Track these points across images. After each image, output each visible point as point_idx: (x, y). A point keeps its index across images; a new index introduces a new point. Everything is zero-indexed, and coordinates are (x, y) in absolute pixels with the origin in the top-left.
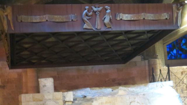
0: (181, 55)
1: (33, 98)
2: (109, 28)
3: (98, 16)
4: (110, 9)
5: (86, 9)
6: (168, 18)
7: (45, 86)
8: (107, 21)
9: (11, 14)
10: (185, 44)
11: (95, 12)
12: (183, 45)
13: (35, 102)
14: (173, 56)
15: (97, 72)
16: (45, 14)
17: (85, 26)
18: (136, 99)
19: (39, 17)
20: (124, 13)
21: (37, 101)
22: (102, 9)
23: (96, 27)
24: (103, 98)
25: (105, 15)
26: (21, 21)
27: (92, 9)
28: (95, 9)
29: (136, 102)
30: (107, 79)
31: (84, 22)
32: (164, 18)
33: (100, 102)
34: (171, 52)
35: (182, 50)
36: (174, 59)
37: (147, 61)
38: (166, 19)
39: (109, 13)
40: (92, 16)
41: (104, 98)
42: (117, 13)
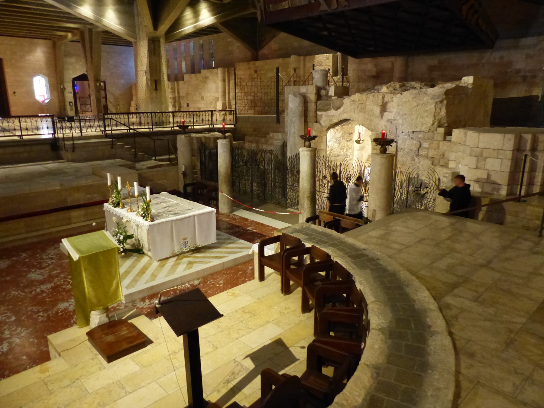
30: (509, 70)
33: (352, 99)
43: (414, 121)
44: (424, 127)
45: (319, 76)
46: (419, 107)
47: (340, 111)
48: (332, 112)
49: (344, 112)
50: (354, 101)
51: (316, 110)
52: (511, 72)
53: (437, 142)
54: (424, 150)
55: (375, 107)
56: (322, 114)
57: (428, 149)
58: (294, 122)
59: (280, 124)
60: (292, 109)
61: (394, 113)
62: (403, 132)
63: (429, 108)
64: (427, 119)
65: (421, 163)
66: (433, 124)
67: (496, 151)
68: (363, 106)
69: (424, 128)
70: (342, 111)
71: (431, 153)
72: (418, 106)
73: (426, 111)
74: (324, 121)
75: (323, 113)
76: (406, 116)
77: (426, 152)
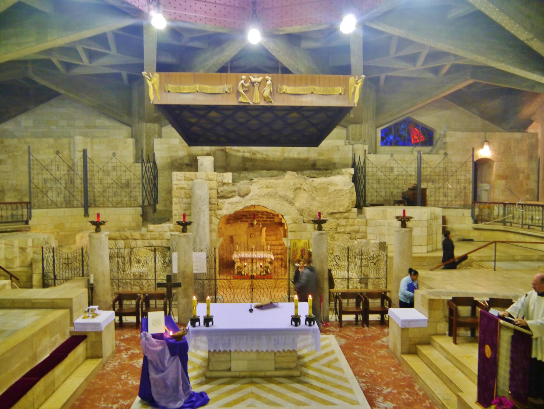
1: (185, 177)
2: (268, 102)
3: (256, 89)
4: (271, 81)
5: (242, 80)
6: (343, 94)
7: (202, 164)
8: (266, 93)
9: (158, 83)
11: (253, 83)
13: (186, 181)
16: (195, 84)
17: (241, 99)
19: (188, 86)
20: (288, 85)
21: (189, 180)
22: (262, 80)
23: (254, 101)
25: (265, 86)
26: (169, 91)
27: (250, 79)
28: (253, 79)
31: (238, 94)
32: (337, 93)
34: (386, 138)
38: (340, 94)
39: (269, 85)
40: (248, 87)
42: (279, 85)
47: (247, 197)
48: (237, 199)
51: (218, 197)
52: (307, 165)
53: (353, 220)
54: (341, 228)
56: (224, 202)
57: (345, 226)
58: (204, 211)
59: (88, 216)
60: (201, 196)
63: (344, 193)
65: (340, 239)
66: (348, 206)
67: (417, 222)
69: (341, 209)
71: (348, 229)
73: (342, 195)
75: (227, 201)
77: (343, 230)
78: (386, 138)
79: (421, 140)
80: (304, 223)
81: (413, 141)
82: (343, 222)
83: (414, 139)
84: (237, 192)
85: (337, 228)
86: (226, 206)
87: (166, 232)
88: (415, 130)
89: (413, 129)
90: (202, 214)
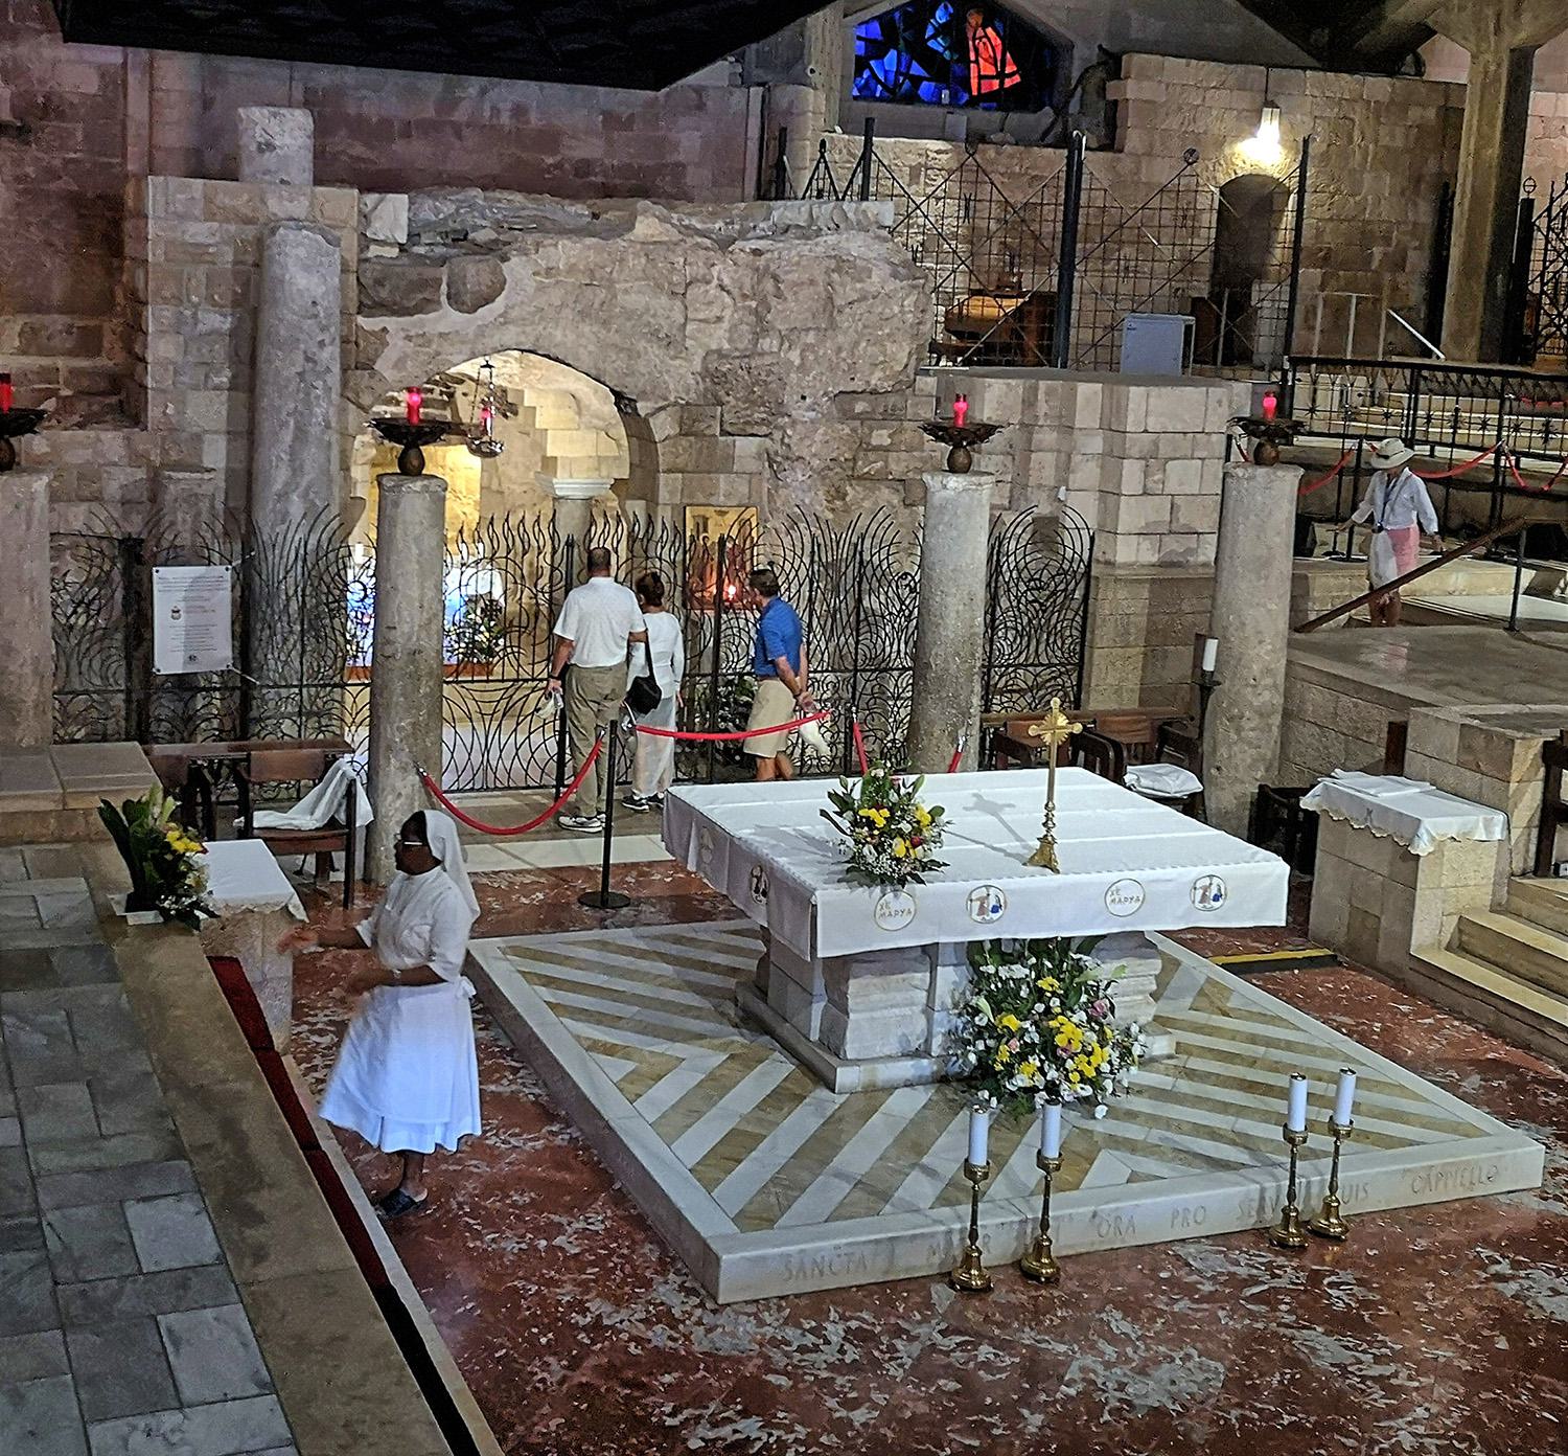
0: (916, 81)
10: (941, 30)
12: (933, 37)
14: (879, 81)
15: (505, 119)
18: (715, 271)
24: (556, 245)
29: (715, 282)
33: (543, 264)
35: (929, 58)
36: (881, 99)
37: (756, 92)
41: (564, 243)
43: (844, 355)
44: (878, 374)
45: (300, 141)
46: (864, 306)
49: (505, 320)
50: (549, 271)
52: (558, 166)
54: (872, 456)
55: (664, 300)
56: (384, 330)
57: (887, 449)
61: (725, 325)
62: (804, 398)
64: (890, 347)
68: (602, 294)
69: (876, 379)
70: (501, 316)
72: (863, 298)
74: (399, 364)
76: (811, 338)
78: (872, 63)
79: (1008, 83)
80: (724, 433)
81: (974, 82)
82: (881, 437)
83: (980, 77)
84: (444, 288)
85: (854, 460)
86: (396, 346)
87: (115, 464)
88: (986, 36)
89: (980, 33)
90: (319, 384)
